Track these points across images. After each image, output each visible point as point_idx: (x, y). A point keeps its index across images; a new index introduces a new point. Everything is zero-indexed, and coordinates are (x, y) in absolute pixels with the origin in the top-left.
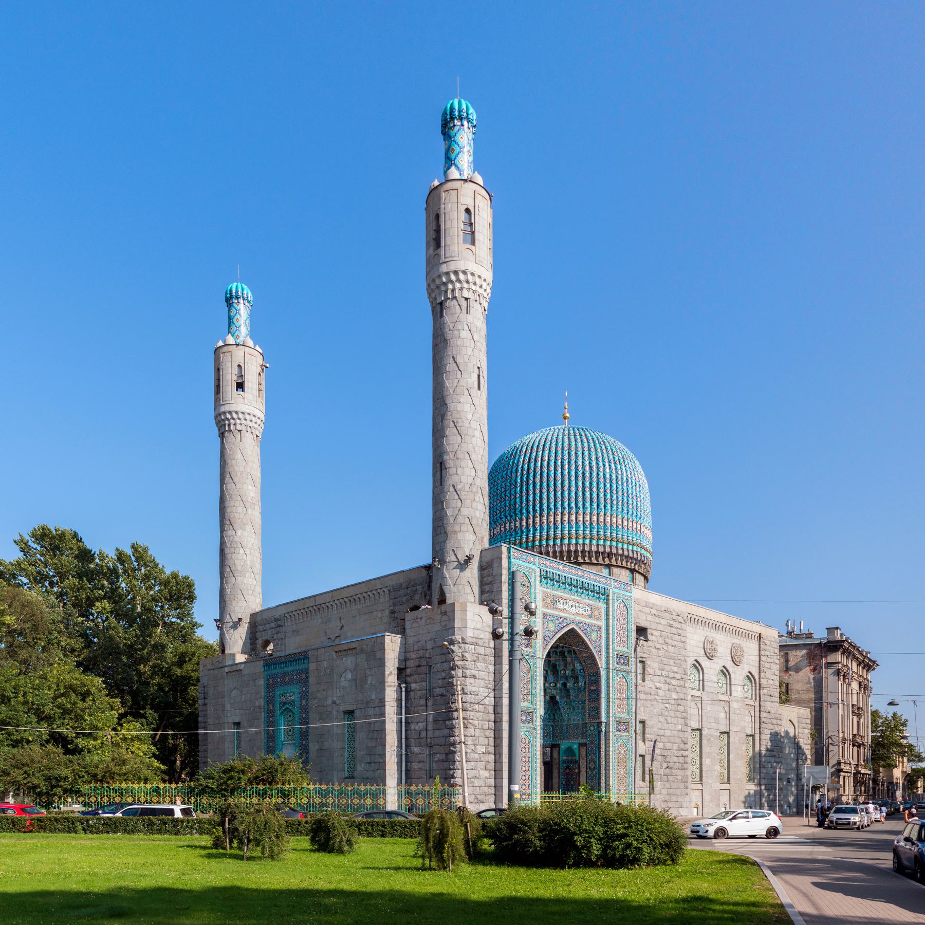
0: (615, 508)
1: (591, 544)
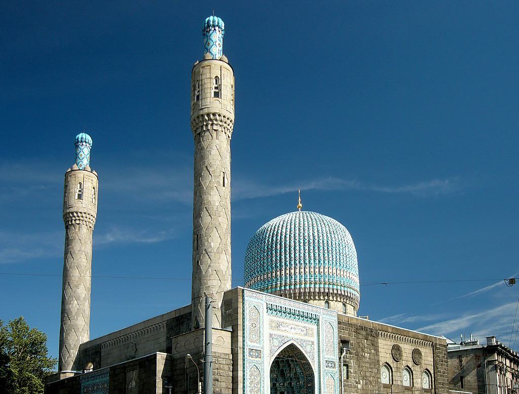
0: (331, 262)
1: (315, 288)
